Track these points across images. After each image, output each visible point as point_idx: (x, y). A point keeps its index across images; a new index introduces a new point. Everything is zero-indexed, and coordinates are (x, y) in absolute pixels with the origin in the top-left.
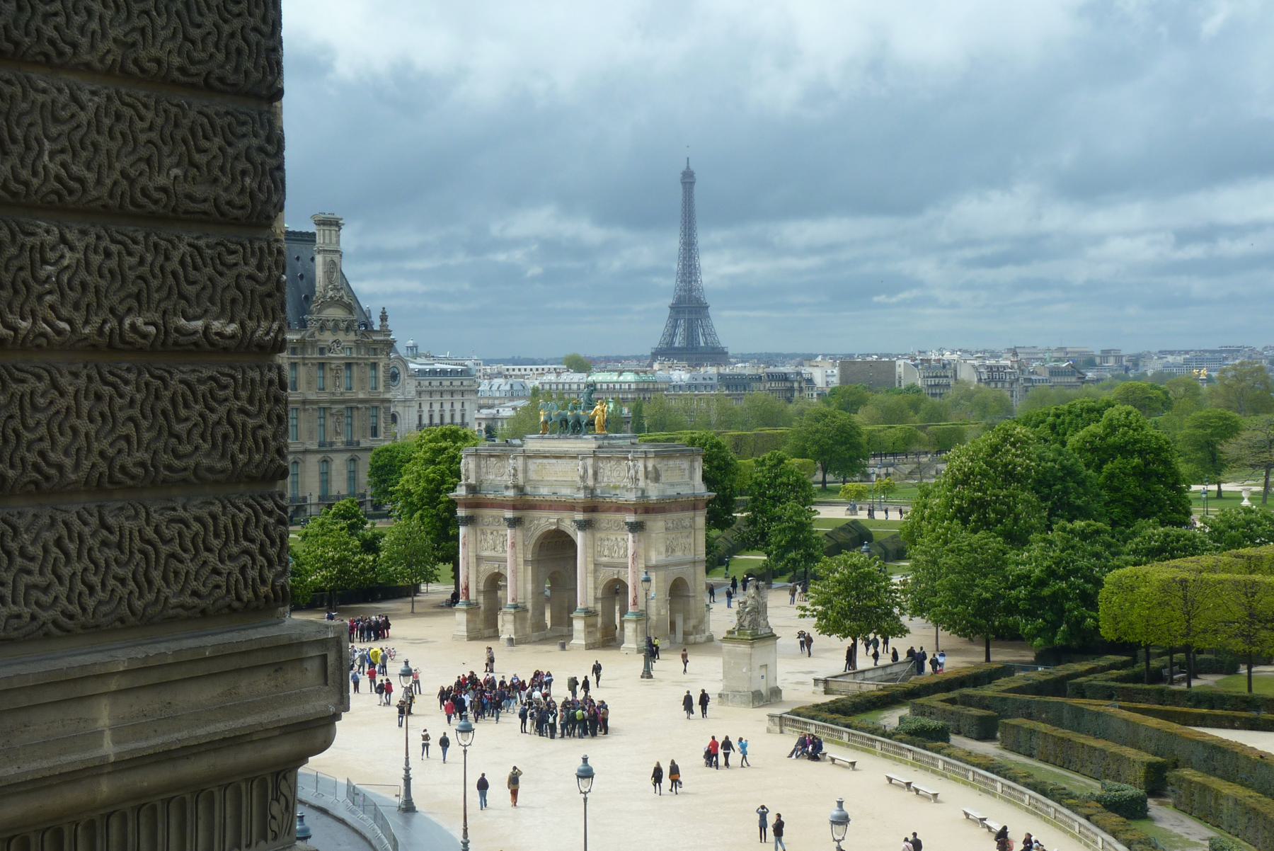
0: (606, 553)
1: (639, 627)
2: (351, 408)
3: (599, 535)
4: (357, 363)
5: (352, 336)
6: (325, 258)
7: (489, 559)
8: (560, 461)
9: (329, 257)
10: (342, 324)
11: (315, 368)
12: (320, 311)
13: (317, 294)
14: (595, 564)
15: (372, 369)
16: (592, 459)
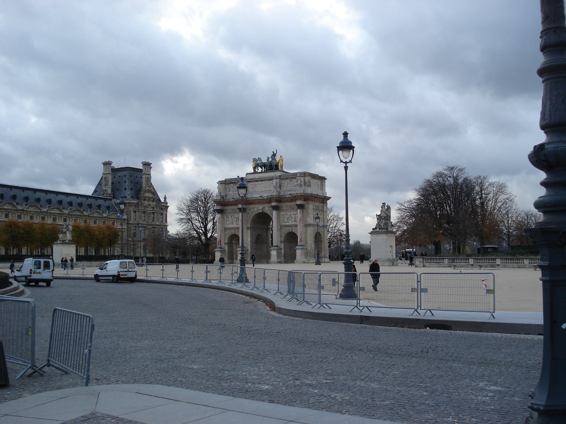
0: (286, 221)
1: (303, 251)
2: (154, 227)
3: (282, 213)
4: (156, 213)
5: (154, 203)
6: (146, 176)
7: (230, 229)
8: (263, 182)
9: (147, 176)
10: (151, 199)
11: (142, 213)
12: (144, 194)
13: (143, 188)
14: (280, 226)
15: (161, 215)
16: (279, 179)
